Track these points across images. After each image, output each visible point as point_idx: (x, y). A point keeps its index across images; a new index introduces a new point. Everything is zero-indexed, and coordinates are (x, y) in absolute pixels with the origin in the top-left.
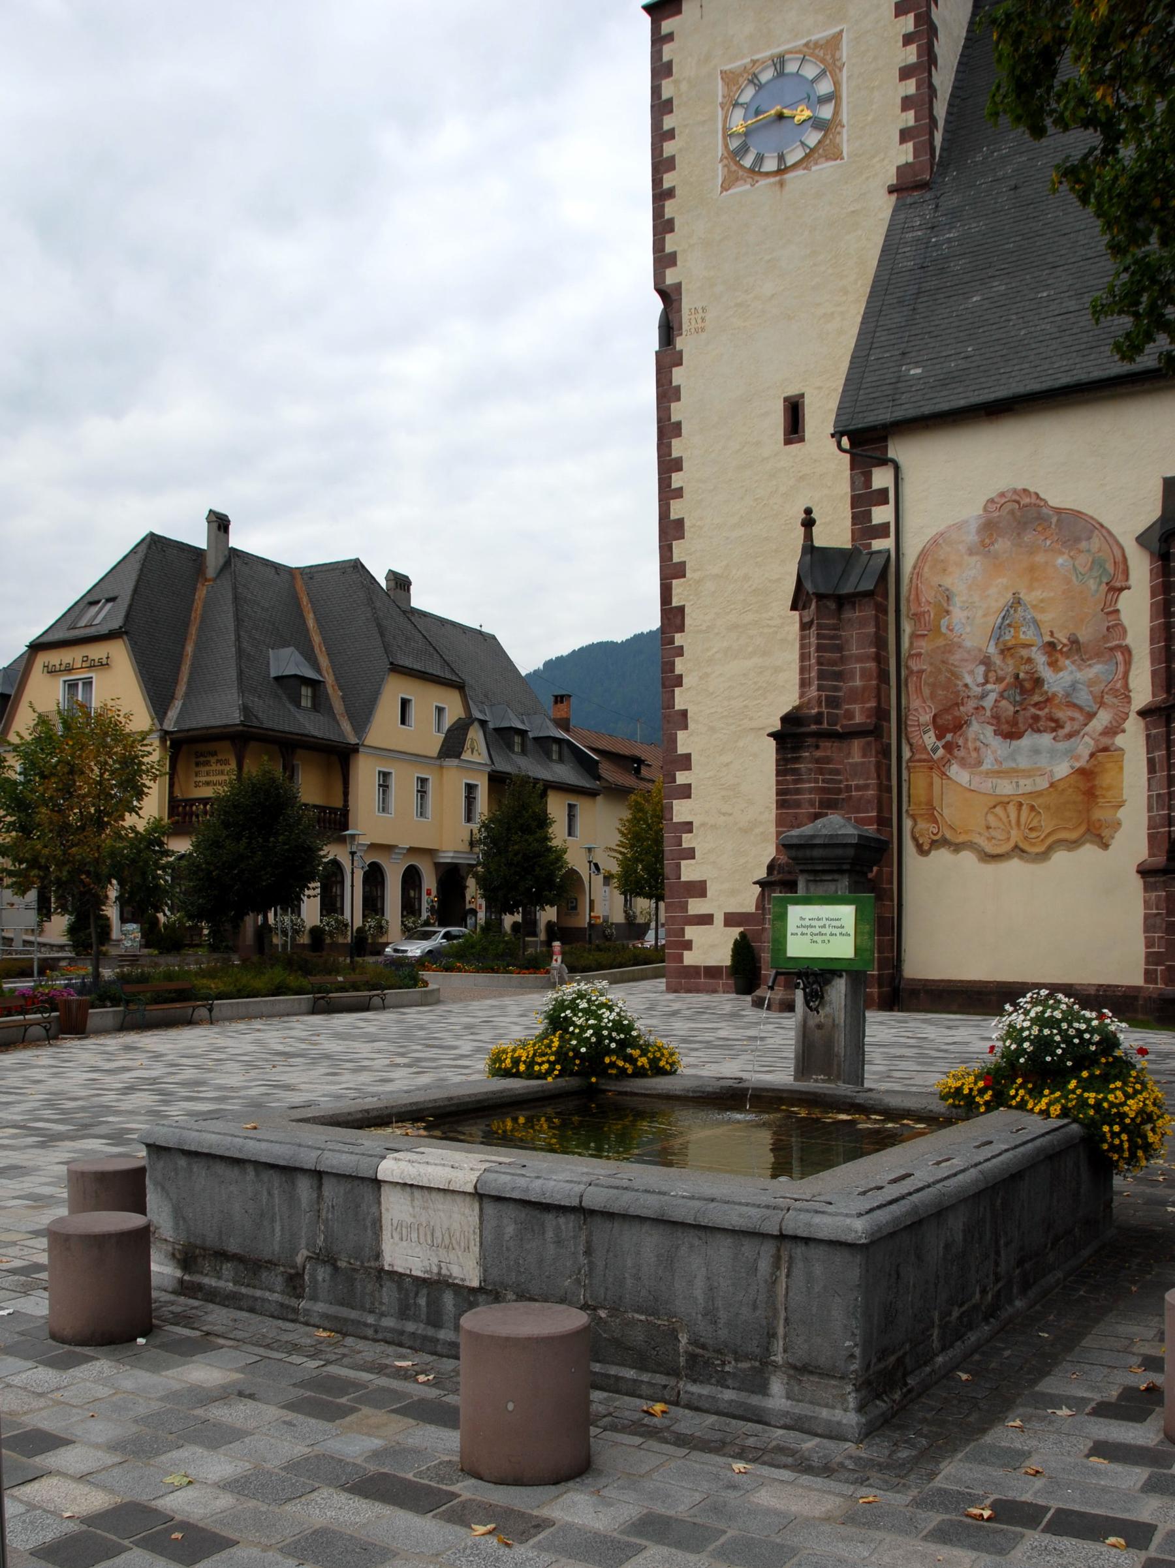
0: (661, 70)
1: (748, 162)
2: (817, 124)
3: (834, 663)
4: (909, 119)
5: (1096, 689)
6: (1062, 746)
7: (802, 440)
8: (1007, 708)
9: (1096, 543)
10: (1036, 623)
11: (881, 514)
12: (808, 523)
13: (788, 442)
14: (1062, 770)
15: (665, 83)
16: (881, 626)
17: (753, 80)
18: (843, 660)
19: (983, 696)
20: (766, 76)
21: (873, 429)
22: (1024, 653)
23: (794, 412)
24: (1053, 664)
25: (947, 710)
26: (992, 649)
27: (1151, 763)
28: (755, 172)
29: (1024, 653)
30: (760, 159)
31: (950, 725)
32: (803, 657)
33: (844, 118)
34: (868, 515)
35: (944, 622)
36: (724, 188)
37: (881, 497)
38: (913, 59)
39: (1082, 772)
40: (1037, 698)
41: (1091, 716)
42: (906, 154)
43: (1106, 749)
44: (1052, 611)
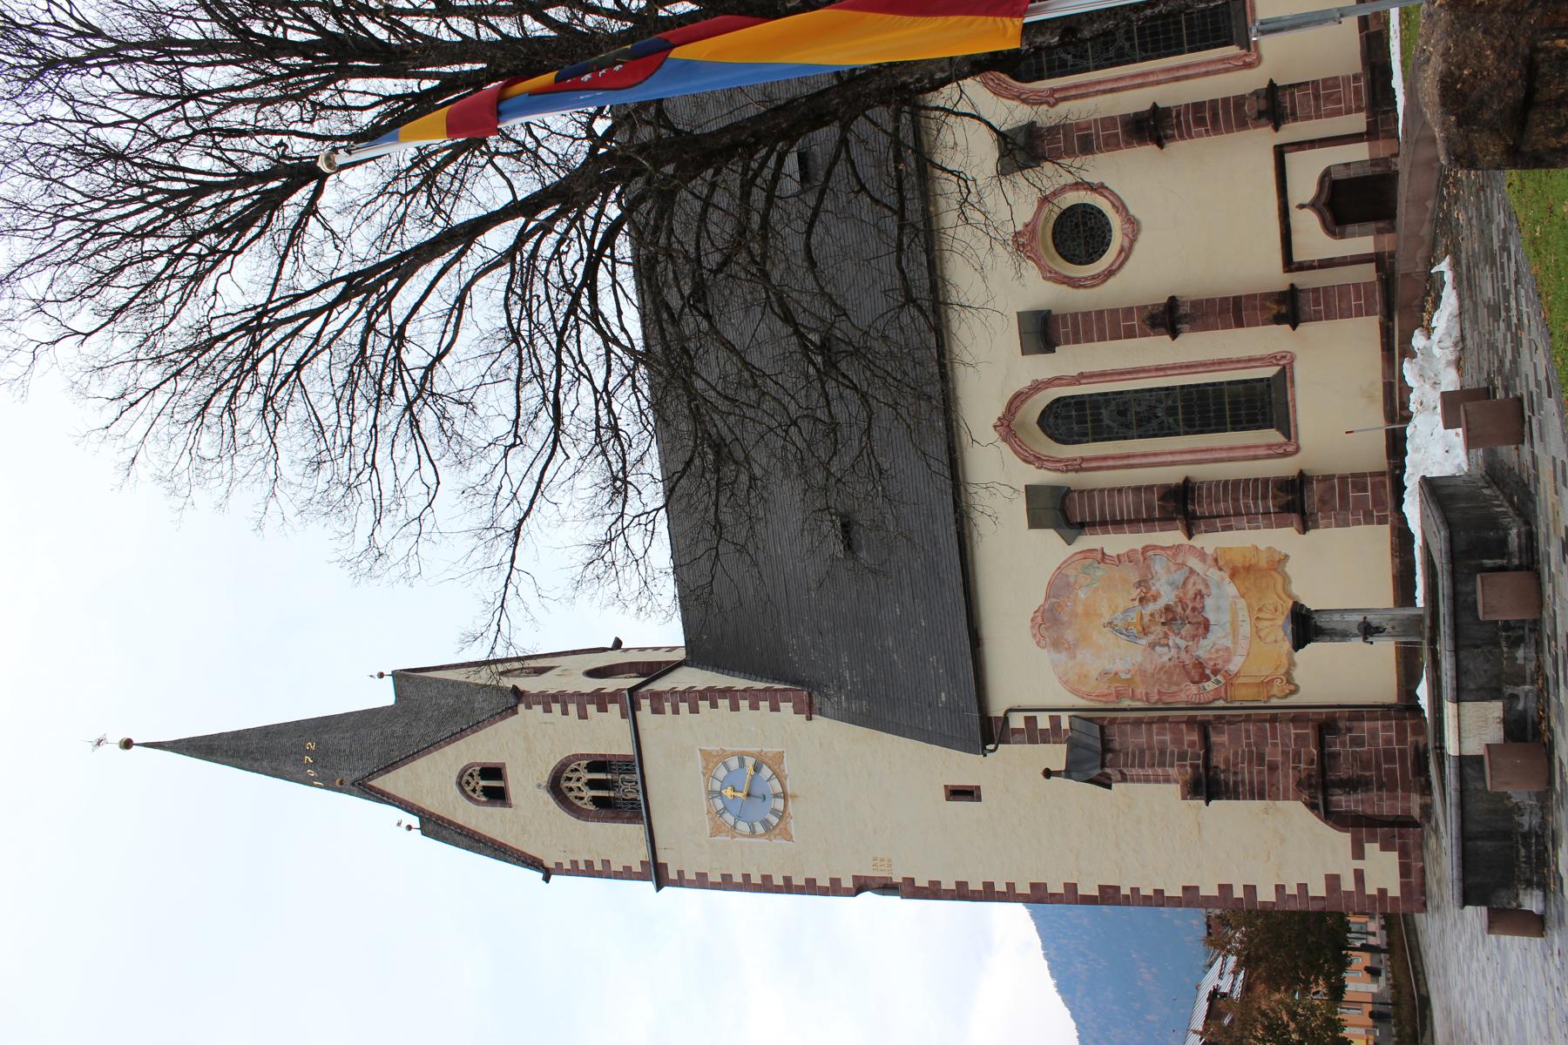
0: (701, 882)
1: (774, 820)
2: (757, 768)
3: (1153, 756)
4: (764, 705)
5: (1173, 568)
6: (1214, 590)
7: (978, 788)
8: (1187, 629)
9: (1070, 572)
10: (1126, 611)
11: (1043, 722)
12: (1048, 774)
13: (979, 799)
14: (1231, 589)
15: (711, 879)
16: (1125, 722)
17: (720, 814)
18: (1151, 748)
19: (1178, 647)
20: (719, 804)
21: (982, 726)
22: (1146, 619)
23: (960, 793)
24: (1155, 599)
25: (1188, 673)
26: (1144, 641)
27: (1225, 529)
28: (782, 816)
29: (1146, 619)
30: (774, 812)
31: (1200, 672)
32: (1147, 780)
33: (756, 749)
34: (1043, 731)
35: (1123, 676)
36: (790, 839)
37: (1031, 722)
38: (726, 702)
39: (1233, 576)
40: (1179, 610)
41: (1192, 571)
42: (787, 708)
43: (1216, 560)
44: (1116, 601)
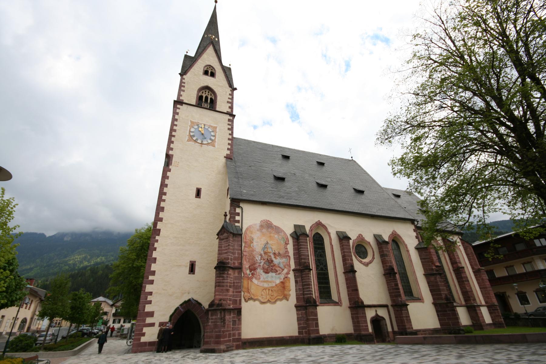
6: (278, 276)
9: (282, 234)
14: (278, 282)
19: (260, 263)
24: (275, 257)
25: (252, 265)
26: (262, 252)
31: (253, 269)
35: (252, 245)
39: (282, 282)
41: (283, 270)
43: (286, 278)
